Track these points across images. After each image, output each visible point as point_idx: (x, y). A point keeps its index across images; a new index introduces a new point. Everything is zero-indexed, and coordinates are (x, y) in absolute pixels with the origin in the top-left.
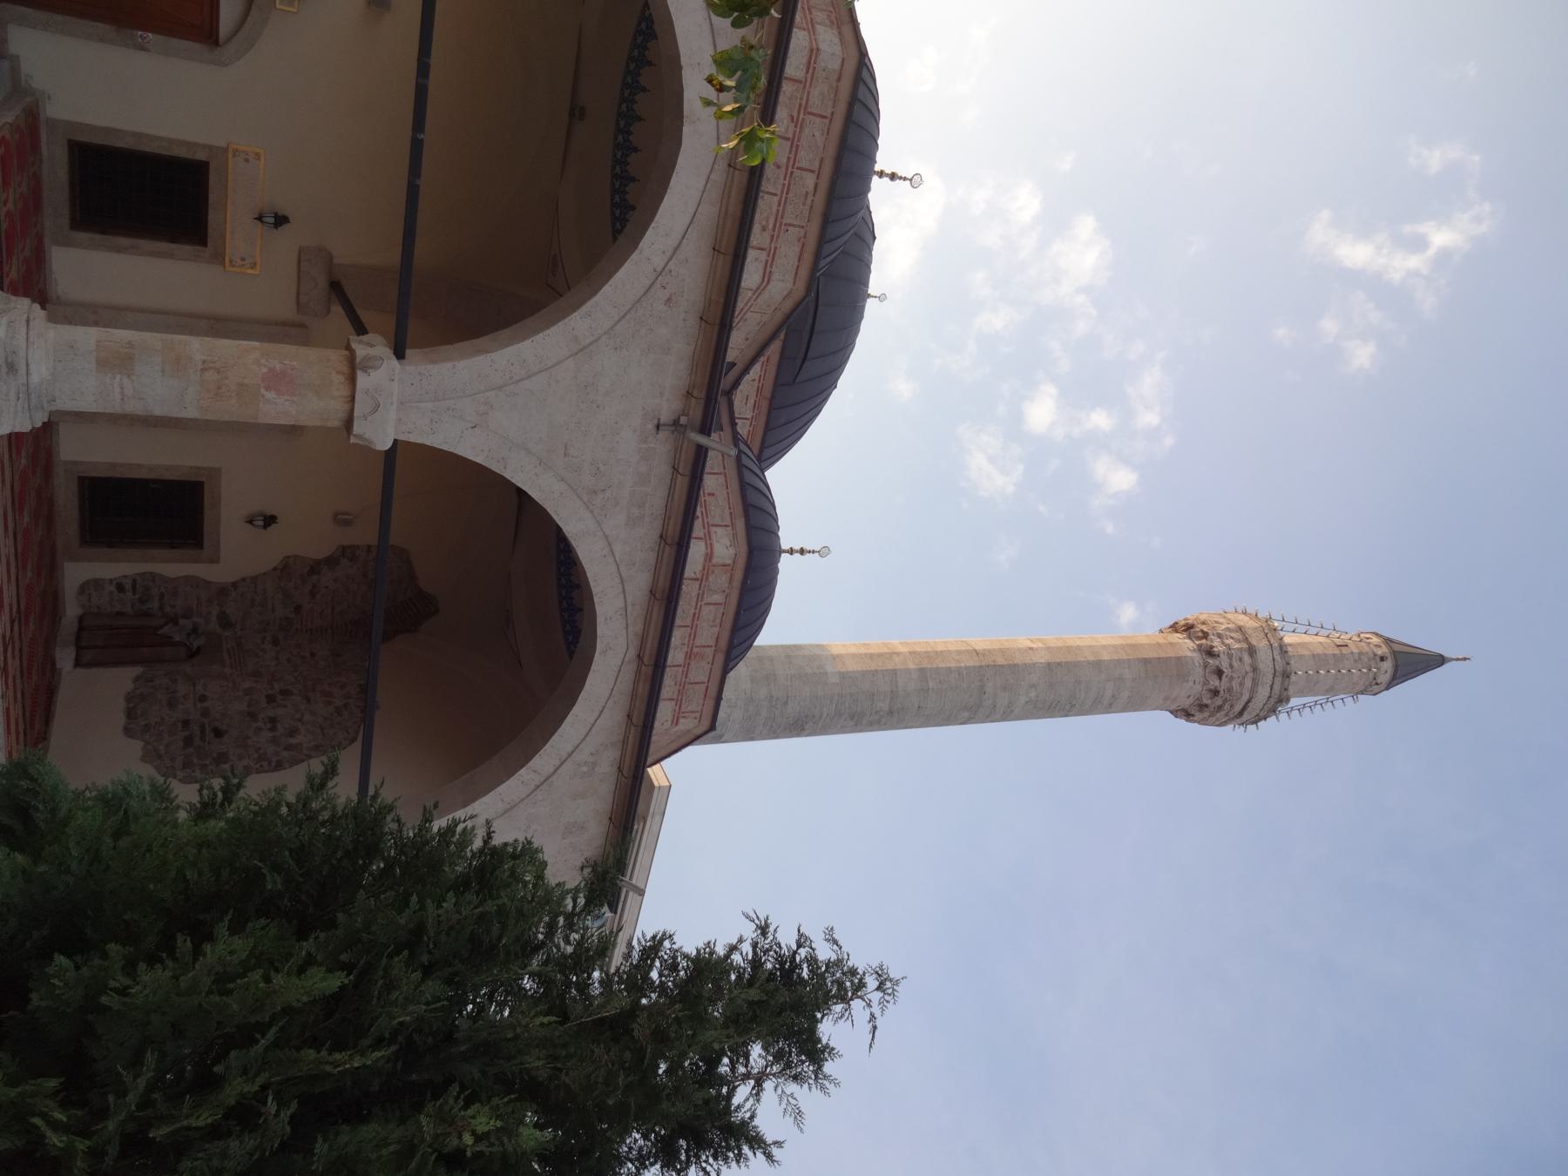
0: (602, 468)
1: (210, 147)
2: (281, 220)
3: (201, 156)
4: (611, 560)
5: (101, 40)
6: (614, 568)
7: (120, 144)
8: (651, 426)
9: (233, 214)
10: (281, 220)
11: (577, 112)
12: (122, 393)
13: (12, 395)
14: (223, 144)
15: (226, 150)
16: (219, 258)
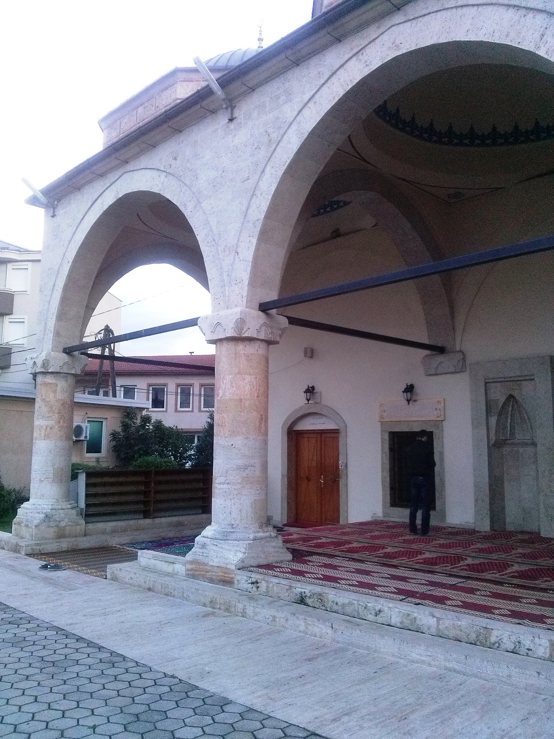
0: (256, 145)
1: (382, 431)
2: (410, 389)
3: (387, 436)
4: (317, 96)
5: (347, 485)
6: (325, 88)
7: (388, 479)
8: (232, 126)
9: (413, 418)
10: (410, 389)
11: (337, 234)
12: (223, 484)
13: (215, 548)
14: (380, 423)
15: (382, 423)
16: (439, 423)
